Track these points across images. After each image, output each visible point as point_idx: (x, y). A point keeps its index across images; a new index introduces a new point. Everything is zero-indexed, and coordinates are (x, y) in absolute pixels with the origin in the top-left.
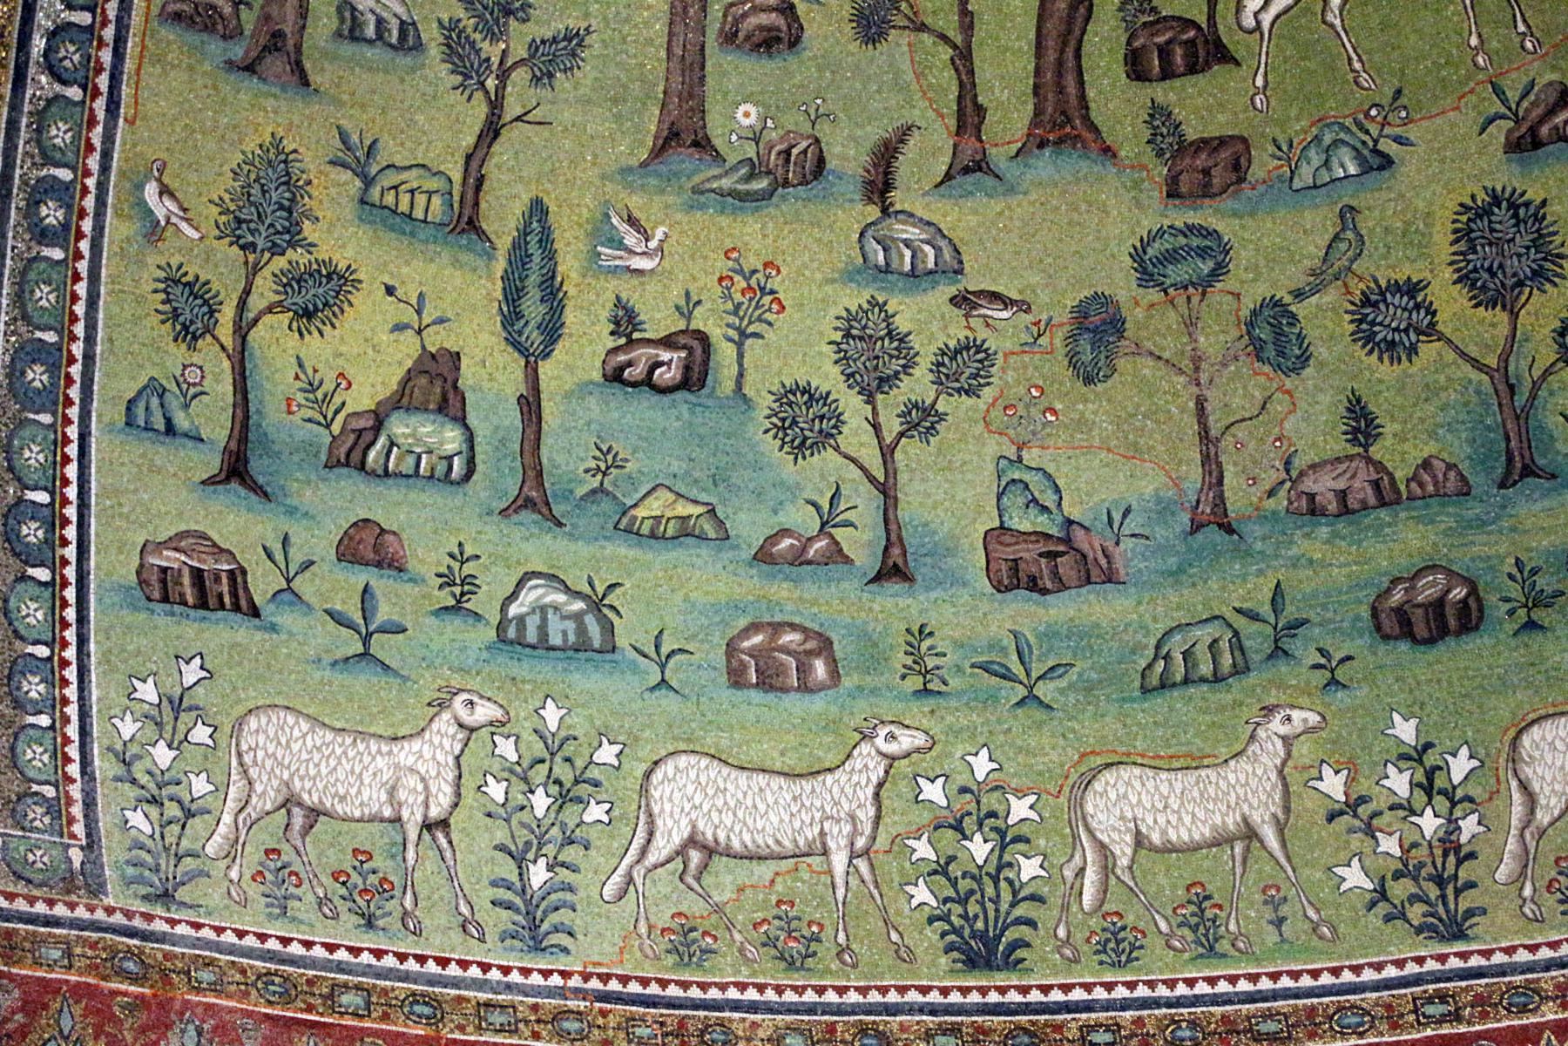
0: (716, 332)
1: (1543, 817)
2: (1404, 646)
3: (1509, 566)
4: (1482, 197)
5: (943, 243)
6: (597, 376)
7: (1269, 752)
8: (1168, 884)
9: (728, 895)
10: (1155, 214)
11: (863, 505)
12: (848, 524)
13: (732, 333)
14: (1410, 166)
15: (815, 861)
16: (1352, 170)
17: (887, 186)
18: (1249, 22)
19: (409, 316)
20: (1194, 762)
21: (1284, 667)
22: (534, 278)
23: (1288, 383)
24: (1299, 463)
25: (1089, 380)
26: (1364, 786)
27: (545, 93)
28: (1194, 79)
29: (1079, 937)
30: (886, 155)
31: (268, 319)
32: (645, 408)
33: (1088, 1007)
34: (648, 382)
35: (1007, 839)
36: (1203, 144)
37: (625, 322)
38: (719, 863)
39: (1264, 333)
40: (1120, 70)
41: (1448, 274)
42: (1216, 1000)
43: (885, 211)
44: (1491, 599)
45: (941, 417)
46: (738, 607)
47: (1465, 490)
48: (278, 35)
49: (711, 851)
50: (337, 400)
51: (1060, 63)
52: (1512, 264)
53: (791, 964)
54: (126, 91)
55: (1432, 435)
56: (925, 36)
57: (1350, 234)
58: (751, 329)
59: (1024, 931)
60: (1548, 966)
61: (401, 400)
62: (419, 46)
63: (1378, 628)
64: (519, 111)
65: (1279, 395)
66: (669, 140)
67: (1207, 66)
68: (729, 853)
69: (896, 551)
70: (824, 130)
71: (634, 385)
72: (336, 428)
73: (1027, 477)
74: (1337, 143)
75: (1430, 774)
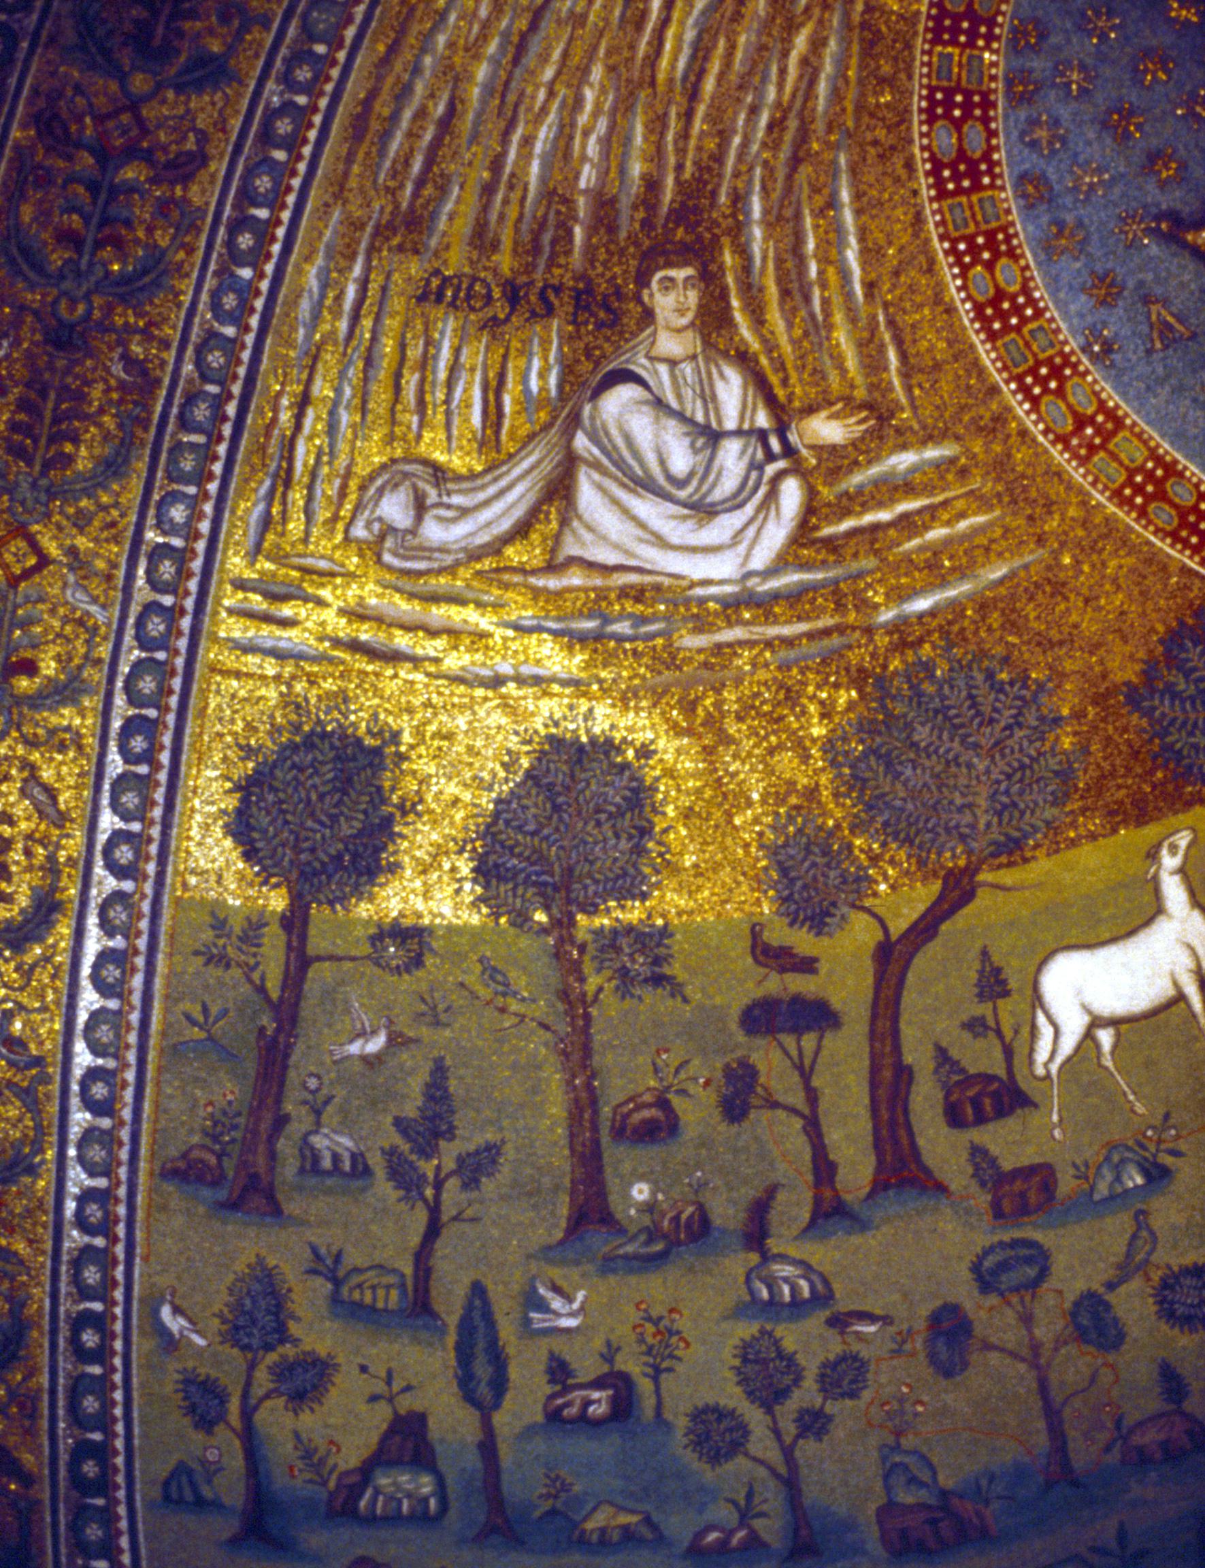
5: (815, 1278)
6: (540, 1418)
12: (762, 1515)
13: (649, 1370)
16: (1139, 1180)
19: (381, 1388)
22: (481, 1344)
23: (1111, 1358)
28: (1002, 1122)
30: (760, 1210)
31: (268, 1404)
37: (559, 1371)
40: (941, 1121)
45: (830, 1418)
48: (254, 1177)
50: (331, 1462)
54: (139, 1235)
57: (1144, 1233)
58: (664, 1365)
61: (379, 1459)
62: (367, 1171)
64: (454, 1212)
65: (1103, 1370)
69: (804, 1532)
71: (571, 1421)
72: (332, 1484)
73: (906, 1460)
74: (1123, 1161)
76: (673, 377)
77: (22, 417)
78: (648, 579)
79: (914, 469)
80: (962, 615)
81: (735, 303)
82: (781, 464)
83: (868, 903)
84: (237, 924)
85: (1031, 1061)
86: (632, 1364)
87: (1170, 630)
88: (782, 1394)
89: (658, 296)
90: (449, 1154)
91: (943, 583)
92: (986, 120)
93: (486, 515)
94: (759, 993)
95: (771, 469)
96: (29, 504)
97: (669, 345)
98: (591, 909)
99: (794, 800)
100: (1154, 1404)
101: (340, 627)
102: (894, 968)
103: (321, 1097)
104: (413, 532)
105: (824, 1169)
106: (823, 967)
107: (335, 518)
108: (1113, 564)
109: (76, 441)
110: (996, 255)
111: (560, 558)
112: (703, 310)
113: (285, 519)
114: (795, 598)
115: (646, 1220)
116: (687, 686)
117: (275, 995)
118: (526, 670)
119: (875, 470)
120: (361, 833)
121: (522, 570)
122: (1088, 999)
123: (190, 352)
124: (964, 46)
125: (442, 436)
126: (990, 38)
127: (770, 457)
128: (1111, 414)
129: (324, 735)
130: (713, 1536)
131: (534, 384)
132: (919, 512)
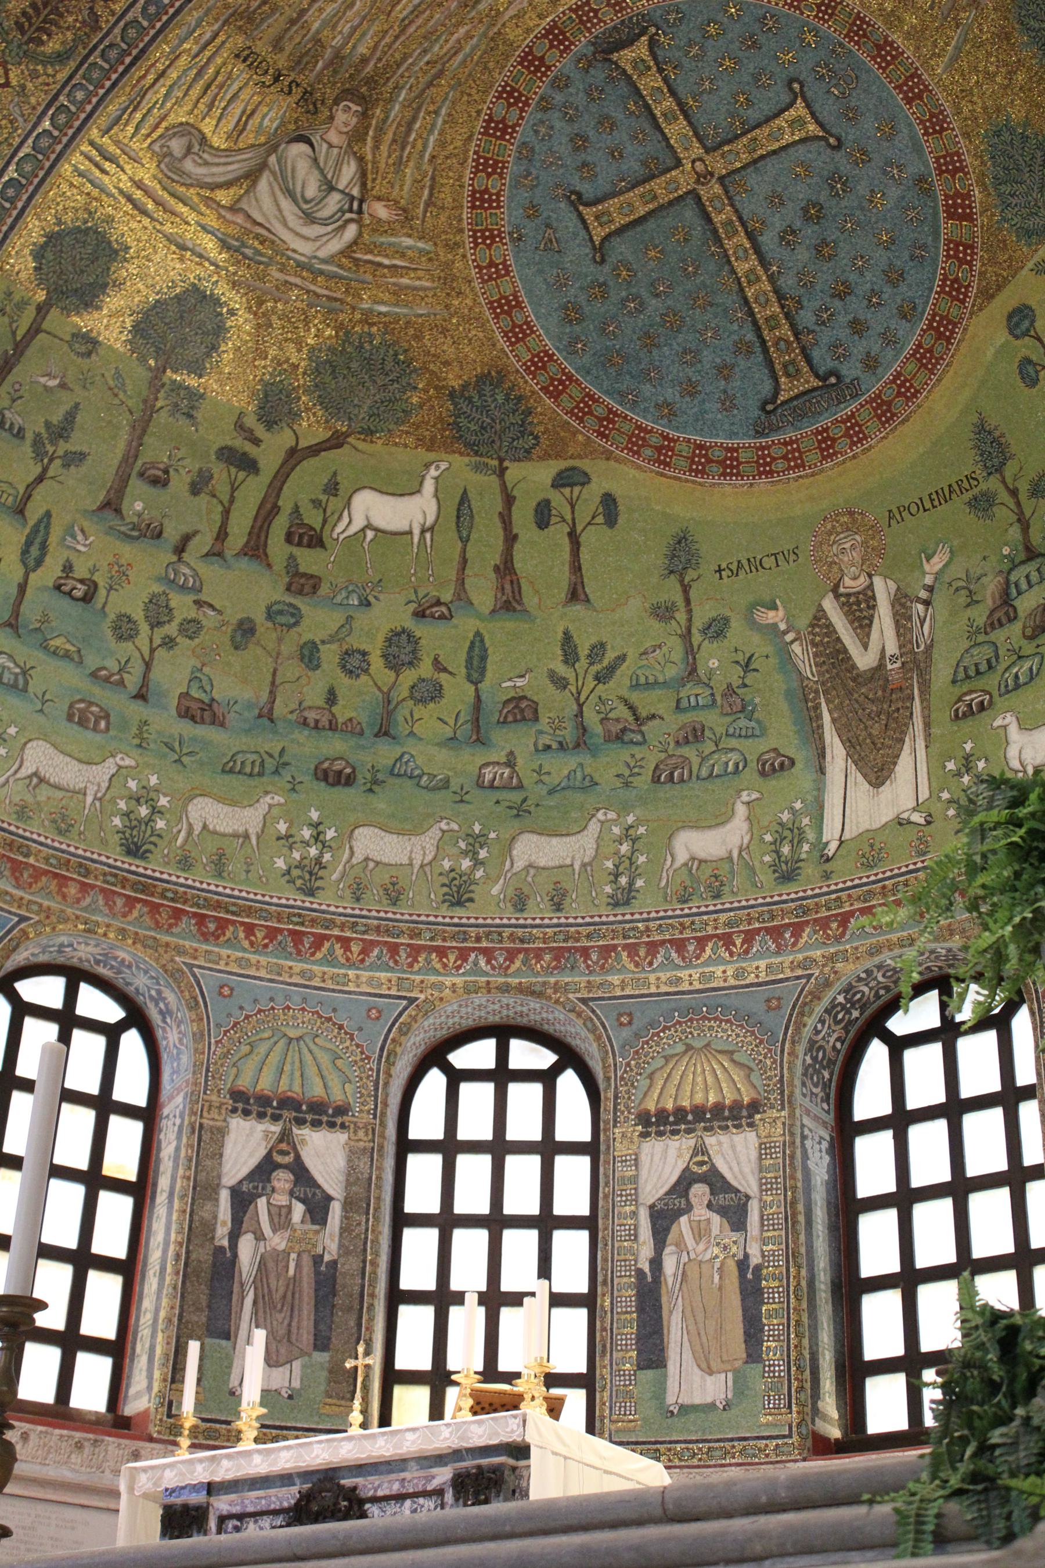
0: (101, 583)
1: (354, 861)
2: (323, 784)
3: (369, 766)
4: (399, 629)
6: (51, 585)
7: (262, 808)
8: (211, 846)
9: (44, 799)
10: (279, 594)
11: (137, 668)
14: (377, 608)
15: (81, 797)
17: (183, 550)
18: (335, 536)
20: (233, 803)
21: (277, 778)
23: (310, 673)
24: (305, 704)
25: (236, 648)
26: (293, 831)
27: (65, 471)
29: (172, 856)
30: (186, 539)
32: (65, 603)
33: (168, 882)
34: (69, 594)
35: (155, 811)
36: (304, 575)
38: (43, 786)
39: (306, 652)
40: (283, 538)
41: (379, 653)
42: (216, 893)
43: (180, 559)
44: (359, 776)
46: (78, 691)
47: (361, 733)
49: (41, 780)
51: (261, 527)
52: (403, 657)
53: (60, 832)
55: (356, 709)
56: (215, 501)
59: (152, 847)
60: (340, 915)
62: (23, 438)
63: (316, 774)
66: (106, 505)
67: (315, 547)
68: (48, 783)
70: (166, 522)
75: (319, 834)
76: (327, 153)
77: (30, 11)
78: (271, 236)
79: (409, 248)
80: (397, 322)
81: (371, 133)
82: (354, 216)
83: (295, 427)
84: (17, 298)
85: (333, 530)
86: (100, 579)
87: (482, 373)
88: (159, 624)
89: (340, 112)
90: (63, 447)
91: (397, 305)
92: (522, 110)
93: (215, 170)
94: (229, 443)
95: (348, 216)
96: (13, 54)
97: (333, 137)
98: (175, 371)
99: (285, 366)
100: (321, 702)
101: (126, 185)
102: (293, 461)
103: (18, 394)
104: (180, 160)
105: (222, 535)
106: (263, 447)
107: (148, 135)
108: (474, 333)
109: (49, 35)
110: (494, 172)
111: (238, 206)
112: (356, 129)
113: (126, 125)
114: (330, 276)
115: (135, 520)
116: (265, 293)
117: (18, 338)
118: (197, 249)
119: (393, 239)
120: (90, 284)
121: (219, 204)
122: (371, 514)
123: (122, 24)
124: (530, 72)
125: (214, 122)
126: (544, 74)
127: (351, 211)
128: (506, 267)
129: (96, 232)
130: (104, 672)
131: (266, 122)
132: (402, 267)
